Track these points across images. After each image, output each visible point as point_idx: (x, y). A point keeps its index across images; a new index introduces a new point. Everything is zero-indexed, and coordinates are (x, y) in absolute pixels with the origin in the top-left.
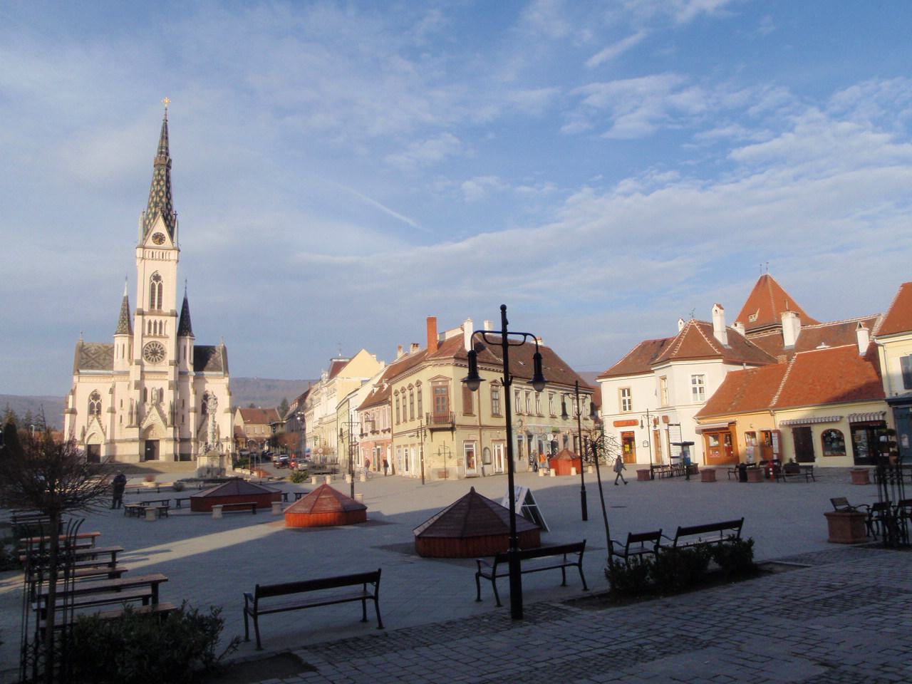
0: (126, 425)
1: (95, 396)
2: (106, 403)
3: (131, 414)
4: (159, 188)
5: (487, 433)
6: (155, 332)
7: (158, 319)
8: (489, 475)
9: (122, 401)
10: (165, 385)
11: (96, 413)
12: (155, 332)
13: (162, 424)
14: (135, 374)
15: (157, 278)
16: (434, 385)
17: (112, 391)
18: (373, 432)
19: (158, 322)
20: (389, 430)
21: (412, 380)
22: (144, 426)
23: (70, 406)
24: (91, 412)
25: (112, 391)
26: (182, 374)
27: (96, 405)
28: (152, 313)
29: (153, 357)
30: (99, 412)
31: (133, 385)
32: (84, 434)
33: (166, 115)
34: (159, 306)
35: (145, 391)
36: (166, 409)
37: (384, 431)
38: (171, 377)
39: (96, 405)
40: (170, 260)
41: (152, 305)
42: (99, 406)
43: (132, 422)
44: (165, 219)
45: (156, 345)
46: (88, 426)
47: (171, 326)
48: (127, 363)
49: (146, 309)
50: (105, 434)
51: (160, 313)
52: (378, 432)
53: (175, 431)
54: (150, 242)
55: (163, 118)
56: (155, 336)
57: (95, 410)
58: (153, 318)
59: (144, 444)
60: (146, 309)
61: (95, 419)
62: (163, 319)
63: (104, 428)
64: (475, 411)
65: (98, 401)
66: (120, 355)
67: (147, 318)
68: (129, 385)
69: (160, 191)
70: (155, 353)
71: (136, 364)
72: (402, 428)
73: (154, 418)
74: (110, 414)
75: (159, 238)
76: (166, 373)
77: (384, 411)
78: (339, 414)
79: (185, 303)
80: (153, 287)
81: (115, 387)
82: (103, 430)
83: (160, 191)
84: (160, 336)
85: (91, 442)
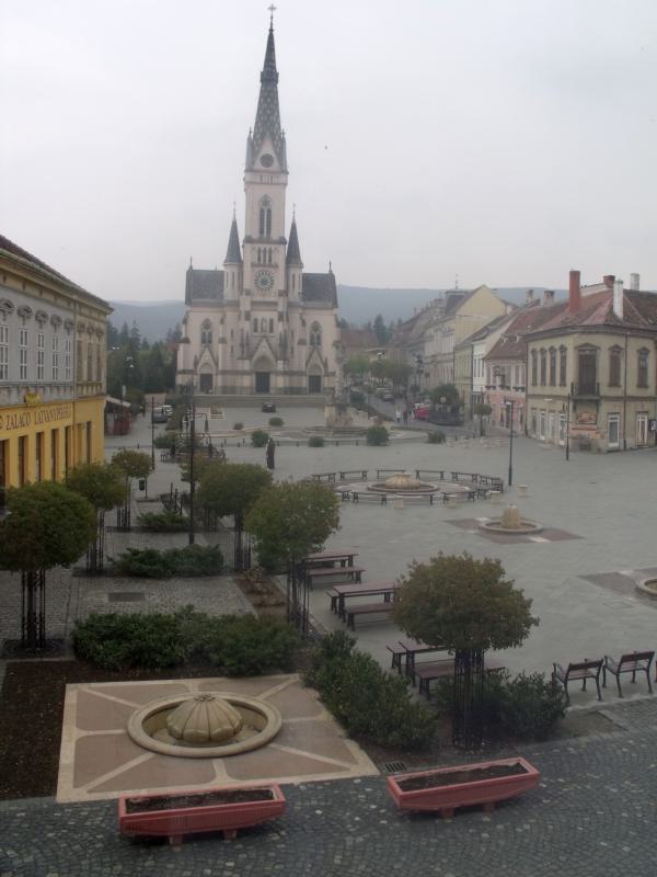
0: (237, 356)
1: (207, 325)
2: (218, 332)
3: (242, 345)
5: (632, 406)
6: (265, 260)
7: (268, 247)
8: (631, 449)
10: (274, 315)
12: (265, 260)
13: (272, 357)
14: (245, 305)
15: (266, 201)
16: (582, 353)
17: (222, 322)
18: (502, 387)
20: (523, 389)
21: (557, 343)
22: (255, 358)
23: (183, 335)
24: (203, 341)
25: (222, 322)
26: (290, 305)
28: (260, 241)
30: (210, 342)
31: (243, 317)
32: (196, 363)
33: (272, 24)
35: (256, 320)
36: (275, 341)
37: (517, 389)
38: (281, 308)
40: (278, 184)
41: (261, 232)
42: (210, 334)
44: (273, 139)
46: (201, 356)
47: (280, 255)
48: (237, 293)
49: (256, 235)
50: (217, 364)
51: (269, 241)
52: (509, 388)
54: (258, 165)
55: (269, 27)
56: (264, 265)
57: (206, 340)
58: (262, 246)
59: (254, 377)
60: (256, 235)
62: (273, 247)
64: (622, 382)
66: (230, 282)
67: (257, 246)
68: (239, 317)
70: (264, 282)
72: (538, 390)
73: (264, 350)
74: (220, 345)
75: (267, 160)
76: (275, 304)
77: (517, 368)
78: (457, 355)
79: (294, 227)
80: (262, 211)
81: (225, 315)
84: (270, 266)
85: (206, 371)
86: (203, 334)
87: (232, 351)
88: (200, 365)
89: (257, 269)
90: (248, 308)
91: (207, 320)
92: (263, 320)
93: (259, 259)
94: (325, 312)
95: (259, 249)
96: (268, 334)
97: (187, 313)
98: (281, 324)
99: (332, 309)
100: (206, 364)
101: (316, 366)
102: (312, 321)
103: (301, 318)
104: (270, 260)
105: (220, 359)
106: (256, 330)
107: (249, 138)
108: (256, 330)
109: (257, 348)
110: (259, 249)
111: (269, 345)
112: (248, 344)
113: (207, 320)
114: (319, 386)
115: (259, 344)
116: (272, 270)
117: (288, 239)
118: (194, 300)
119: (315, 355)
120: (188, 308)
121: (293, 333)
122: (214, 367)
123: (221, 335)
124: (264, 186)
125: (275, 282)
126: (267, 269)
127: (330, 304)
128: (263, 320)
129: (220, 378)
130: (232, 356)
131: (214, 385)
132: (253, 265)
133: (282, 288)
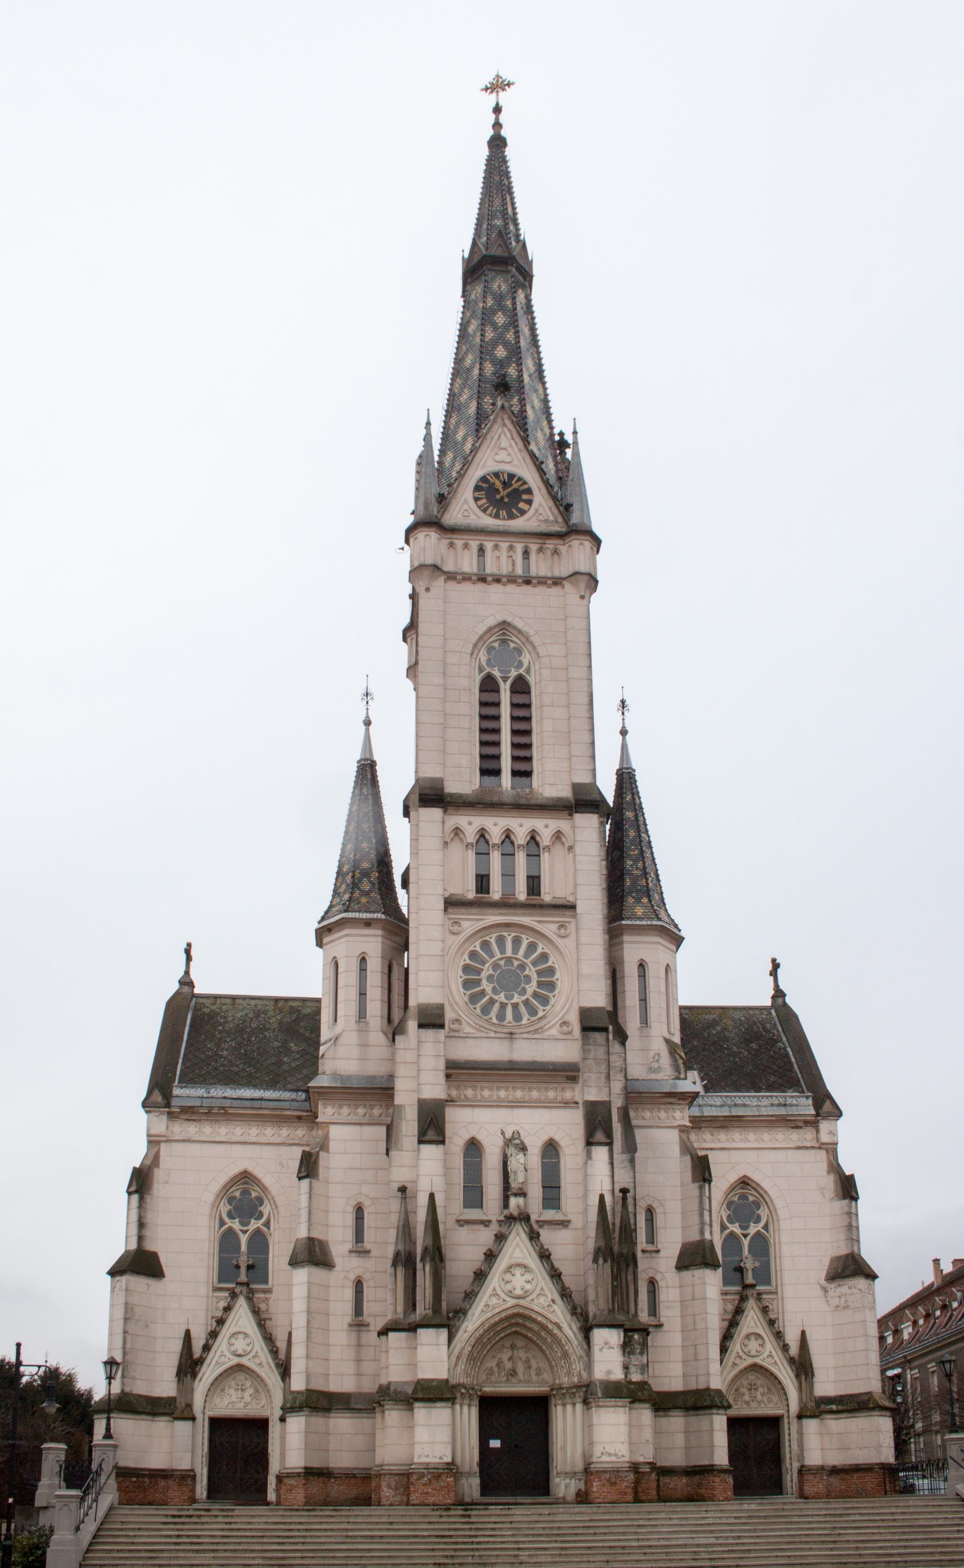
0: (380, 1324)
4: (490, 335)
7: (521, 826)
9: (359, 1212)
11: (243, 1277)
13: (559, 1315)
19: (521, 837)
22: (472, 1324)
27: (244, 1239)
29: (501, 997)
34: (522, 773)
39: (244, 1239)
42: (260, 1242)
43: (411, 1304)
44: (521, 425)
45: (517, 942)
46: (214, 1335)
50: (285, 1370)
53: (626, 1347)
56: (507, 904)
58: (495, 825)
59: (469, 1416)
61: (242, 1302)
63: (281, 1345)
65: (254, 1225)
67: (471, 823)
69: (494, 343)
71: (421, 1026)
73: (519, 1281)
80: (489, 685)
82: (274, 1352)
83: (494, 343)
86: (228, 1241)
87: (358, 1309)
88: (208, 1373)
89: (471, 922)
90: (435, 1088)
91: (245, 1177)
92: (515, 1143)
93: (483, 882)
94: (782, 1137)
95: (482, 835)
96: (534, 1205)
97: (154, 1142)
98: (601, 1153)
99: (813, 1124)
100: (240, 1368)
101: (755, 1368)
102: (733, 1177)
103: (686, 1148)
104: (534, 884)
105: (299, 1336)
106: (474, 1195)
107: (423, 460)
108: (474, 1195)
109: (480, 1276)
110: (482, 835)
111: (545, 1256)
112: (436, 1253)
113: (245, 1177)
114: (777, 1459)
115: (491, 1256)
116: (548, 925)
117: (608, 789)
118: (182, 1093)
119: (752, 1321)
120: (161, 1124)
121: (650, 1211)
122: (271, 1376)
123: (303, 1233)
124: (496, 590)
125: (562, 978)
126: (526, 920)
127: (804, 1106)
128: (515, 1143)
129: (296, 1423)
130: (358, 1324)
131: (275, 1467)
132: (451, 903)
133: (598, 998)
